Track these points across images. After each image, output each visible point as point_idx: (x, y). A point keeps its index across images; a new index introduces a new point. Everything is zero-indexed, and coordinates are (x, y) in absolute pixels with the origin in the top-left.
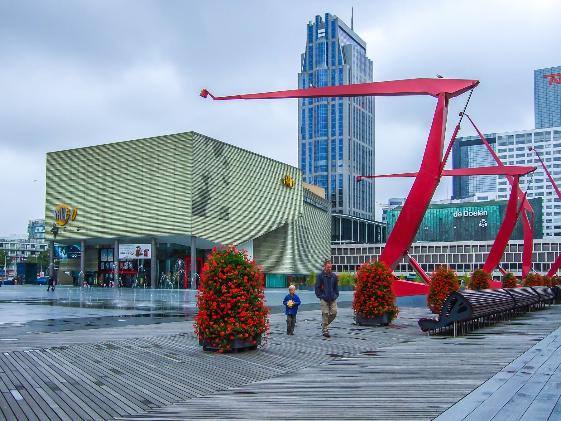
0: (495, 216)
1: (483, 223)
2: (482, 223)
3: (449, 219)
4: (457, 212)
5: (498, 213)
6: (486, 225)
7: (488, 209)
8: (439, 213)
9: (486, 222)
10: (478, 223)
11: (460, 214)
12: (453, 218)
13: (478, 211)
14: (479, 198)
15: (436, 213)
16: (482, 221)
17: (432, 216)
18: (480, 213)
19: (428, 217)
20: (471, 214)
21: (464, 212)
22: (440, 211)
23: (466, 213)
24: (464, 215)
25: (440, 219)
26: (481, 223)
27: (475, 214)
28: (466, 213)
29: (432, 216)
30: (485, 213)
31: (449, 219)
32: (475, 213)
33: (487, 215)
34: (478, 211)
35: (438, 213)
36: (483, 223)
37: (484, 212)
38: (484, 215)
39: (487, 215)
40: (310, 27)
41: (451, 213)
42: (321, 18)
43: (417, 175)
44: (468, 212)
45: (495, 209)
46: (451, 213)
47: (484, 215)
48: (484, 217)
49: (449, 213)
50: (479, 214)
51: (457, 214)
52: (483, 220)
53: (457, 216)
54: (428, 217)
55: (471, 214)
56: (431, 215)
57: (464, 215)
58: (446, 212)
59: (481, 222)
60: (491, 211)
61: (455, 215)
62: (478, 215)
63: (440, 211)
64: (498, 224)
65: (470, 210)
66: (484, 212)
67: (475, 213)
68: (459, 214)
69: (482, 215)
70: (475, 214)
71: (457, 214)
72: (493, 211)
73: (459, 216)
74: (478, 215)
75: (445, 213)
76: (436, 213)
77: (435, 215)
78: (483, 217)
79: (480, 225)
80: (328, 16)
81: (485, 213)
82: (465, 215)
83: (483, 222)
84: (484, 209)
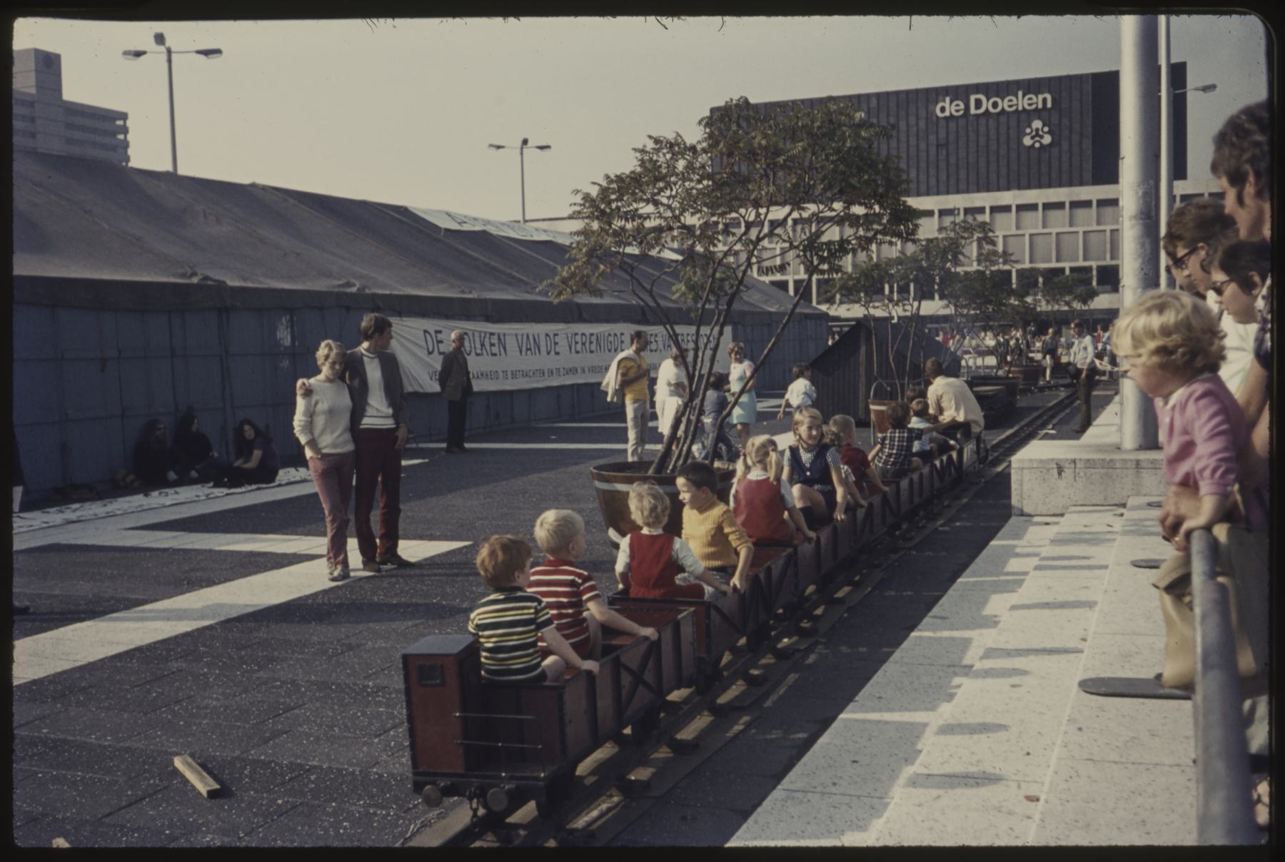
1: (1037, 135)
10: (1021, 134)
11: (958, 108)
20: (995, 105)
24: (973, 111)
26: (1029, 134)
27: (1010, 106)
28: (978, 104)
30: (1045, 100)
33: (1049, 105)
37: (1041, 97)
39: (1049, 105)
47: (1040, 106)
51: (947, 105)
53: (947, 114)
55: (995, 105)
59: (1028, 130)
62: (1020, 108)
68: (953, 108)
70: (1010, 106)
73: (955, 114)
79: (1027, 141)
81: (1045, 100)
83: (1037, 130)
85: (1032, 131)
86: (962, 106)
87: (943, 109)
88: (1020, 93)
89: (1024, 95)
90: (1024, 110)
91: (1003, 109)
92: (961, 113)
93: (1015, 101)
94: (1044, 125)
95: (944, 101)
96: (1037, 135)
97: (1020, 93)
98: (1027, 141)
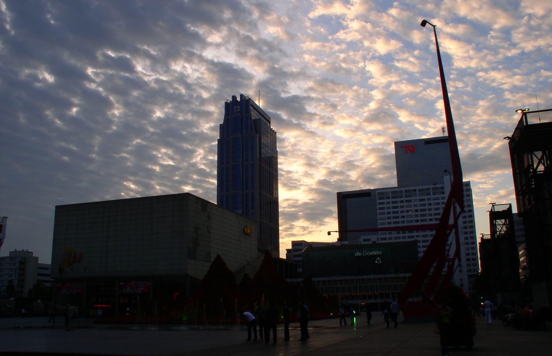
10: (375, 261)
14: (364, 240)
18: (376, 253)
21: (363, 252)
24: (364, 255)
27: (372, 254)
28: (365, 253)
30: (380, 253)
33: (381, 254)
37: (379, 252)
40: (227, 105)
42: (236, 98)
43: (520, 256)
44: (366, 252)
47: (379, 254)
51: (358, 253)
53: (358, 255)
55: (369, 254)
57: (364, 255)
61: (357, 254)
66: (379, 252)
71: (358, 253)
79: (376, 262)
80: (242, 97)
81: (380, 253)
86: (361, 254)
87: (357, 254)
88: (374, 252)
89: (375, 252)
90: (375, 255)
91: (370, 255)
92: (361, 255)
94: (380, 258)
97: (374, 252)
98: (376, 262)
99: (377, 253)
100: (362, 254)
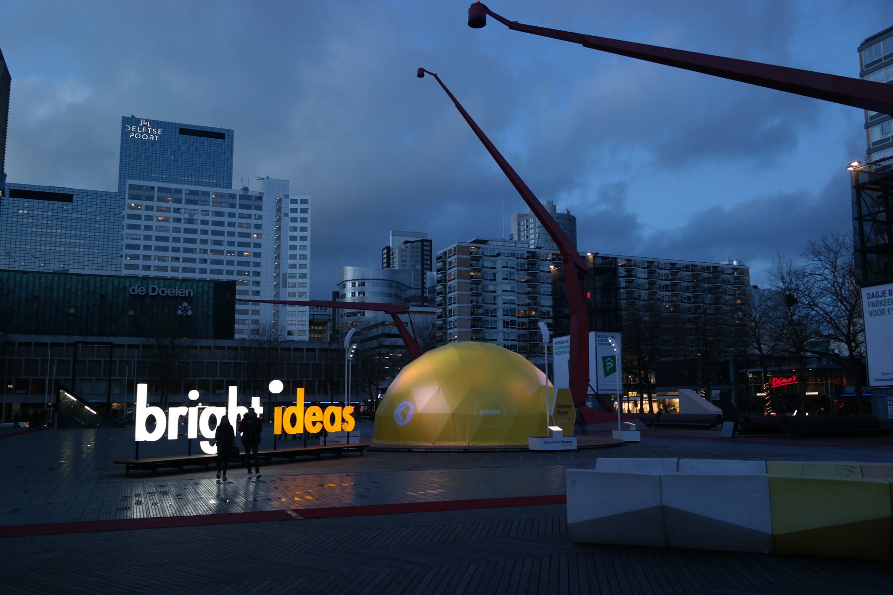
0: (206, 299)
1: (185, 310)
2: (183, 309)
3: (121, 298)
4: (137, 285)
5: (212, 295)
6: (190, 313)
7: (195, 286)
8: (101, 285)
9: (189, 307)
12: (127, 295)
13: (177, 288)
15: (95, 284)
16: (183, 306)
17: (85, 289)
18: (180, 292)
19: (77, 290)
20: (163, 292)
22: (102, 281)
23: (154, 289)
24: (150, 293)
25: (102, 296)
27: (171, 293)
28: (154, 289)
29: (85, 289)
30: (189, 292)
31: (121, 298)
32: (171, 290)
33: (192, 295)
34: (177, 288)
35: (98, 285)
36: (184, 310)
37: (187, 291)
38: (187, 296)
39: (192, 295)
41: (125, 287)
45: (206, 287)
46: (125, 287)
47: (187, 296)
48: (187, 299)
49: (121, 286)
50: (178, 293)
51: (136, 288)
52: (185, 304)
53: (136, 293)
54: (77, 290)
56: (83, 287)
57: (150, 293)
58: (116, 283)
59: (180, 307)
60: (200, 290)
61: (134, 290)
62: (176, 295)
63: (102, 281)
64: (211, 312)
65: (162, 285)
66: (187, 291)
67: (171, 290)
69: (184, 295)
70: (171, 293)
71: (136, 288)
72: (203, 290)
73: (141, 294)
74: (176, 295)
75: (113, 286)
76: (95, 284)
77: (92, 288)
78: (184, 299)
79: (179, 312)
81: (189, 292)
82: (152, 292)
84: (187, 286)
85: (182, 308)
87: (134, 290)
92: (144, 293)
93: (174, 292)
95: (135, 286)
96: (185, 310)
98: (179, 312)
99: (184, 292)
100: (147, 290)
